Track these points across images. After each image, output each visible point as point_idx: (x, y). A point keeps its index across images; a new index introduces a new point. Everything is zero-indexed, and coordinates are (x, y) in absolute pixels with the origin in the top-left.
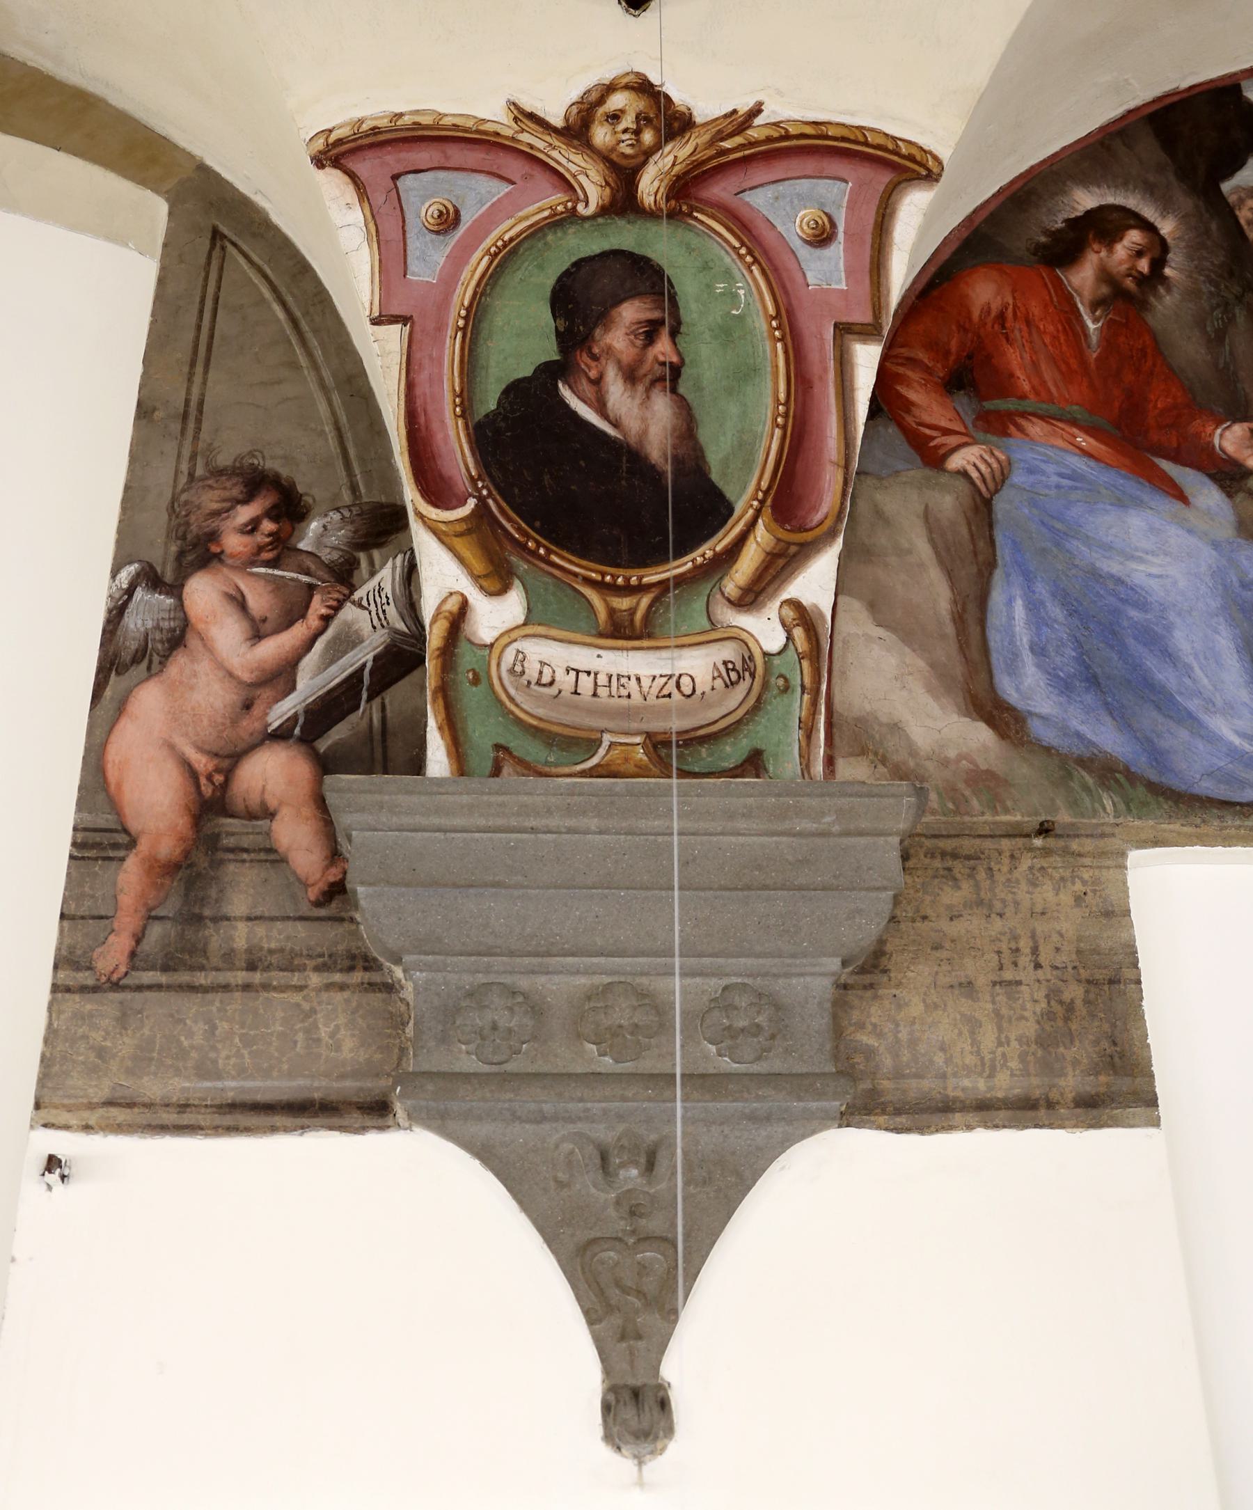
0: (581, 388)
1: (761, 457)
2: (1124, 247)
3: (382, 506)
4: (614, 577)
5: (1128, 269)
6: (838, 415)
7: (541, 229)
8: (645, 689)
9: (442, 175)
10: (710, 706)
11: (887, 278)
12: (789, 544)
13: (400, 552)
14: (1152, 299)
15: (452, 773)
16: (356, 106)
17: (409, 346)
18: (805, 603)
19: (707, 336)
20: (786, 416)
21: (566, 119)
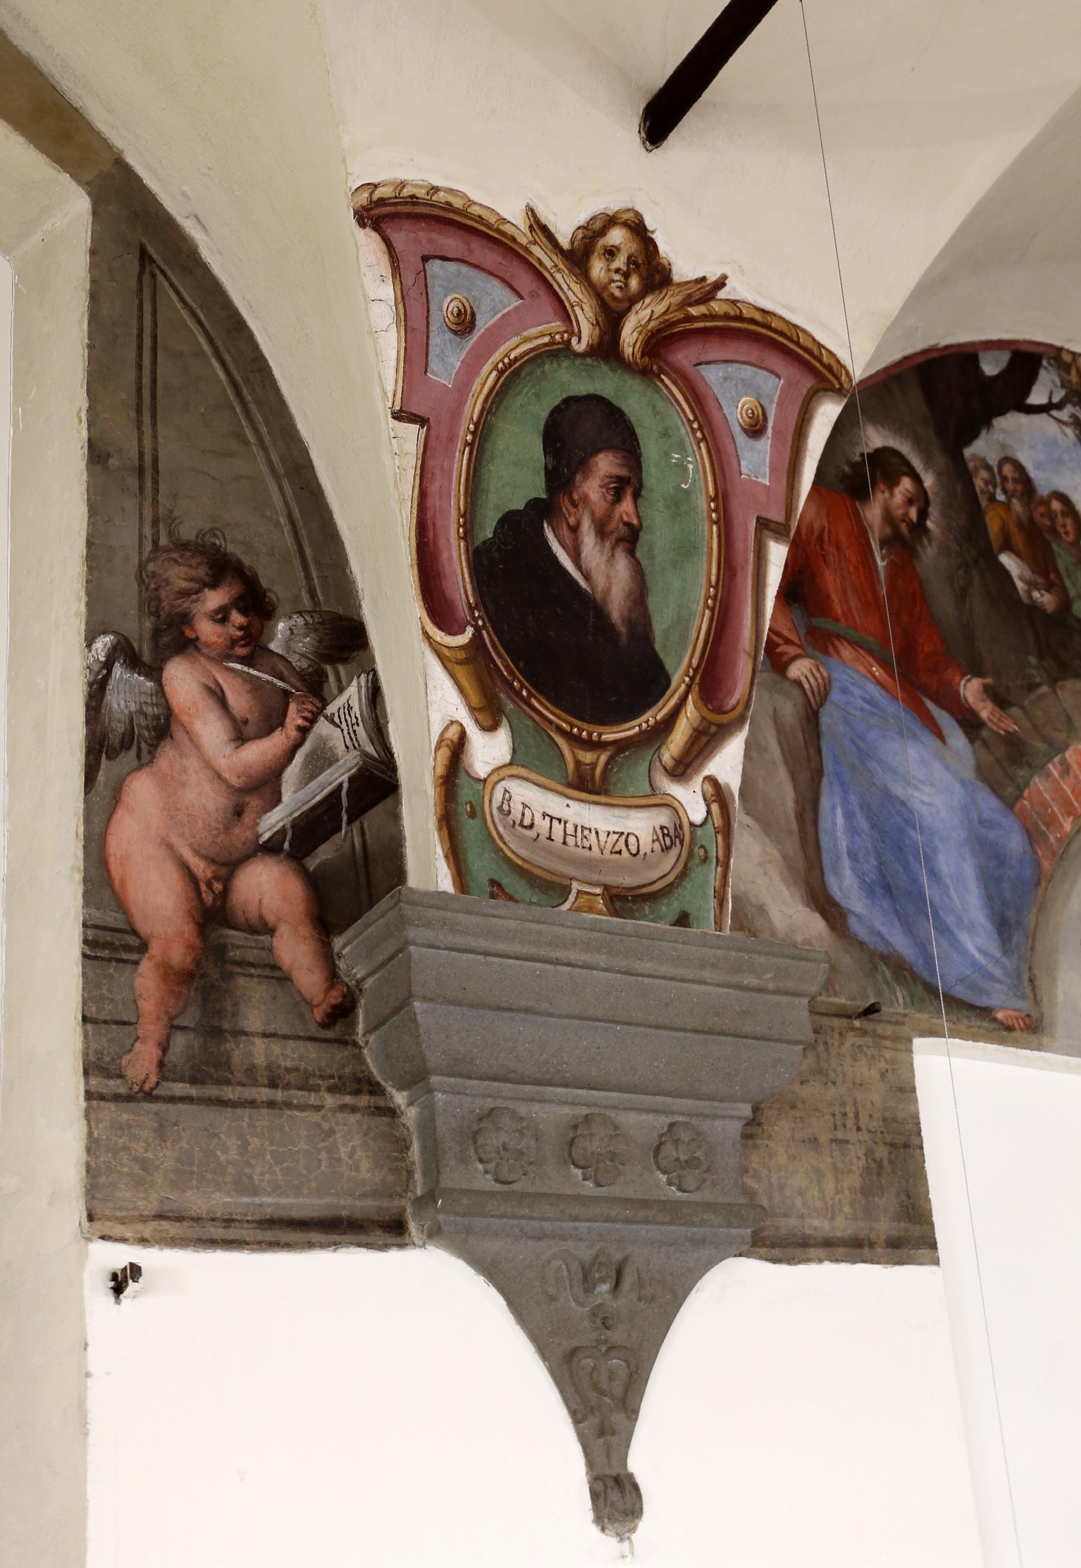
0: (561, 533)
4: (581, 730)
6: (752, 607)
7: (541, 354)
8: (602, 844)
9: (464, 269)
11: (799, 483)
12: (710, 723)
16: (401, 165)
17: (424, 452)
18: (720, 781)
20: (715, 599)
21: (572, 242)
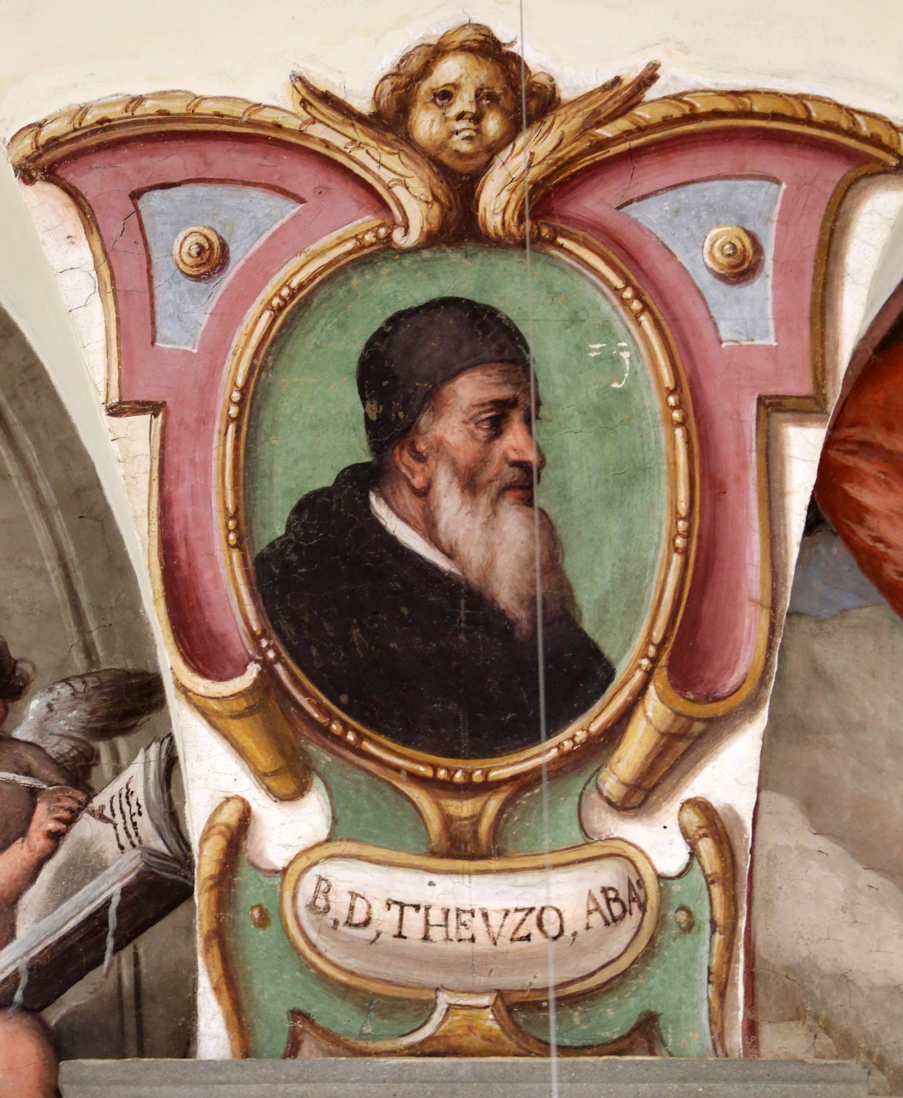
0: (400, 502)
1: (652, 595)
3: (128, 674)
4: (451, 771)
6: (762, 533)
7: (342, 270)
8: (495, 929)
9: (201, 190)
10: (584, 952)
11: (835, 327)
12: (692, 719)
13: (155, 740)
15: (233, 1051)
16: (76, 86)
17: (163, 447)
18: (715, 804)
19: (577, 422)
20: (688, 535)
21: (376, 100)
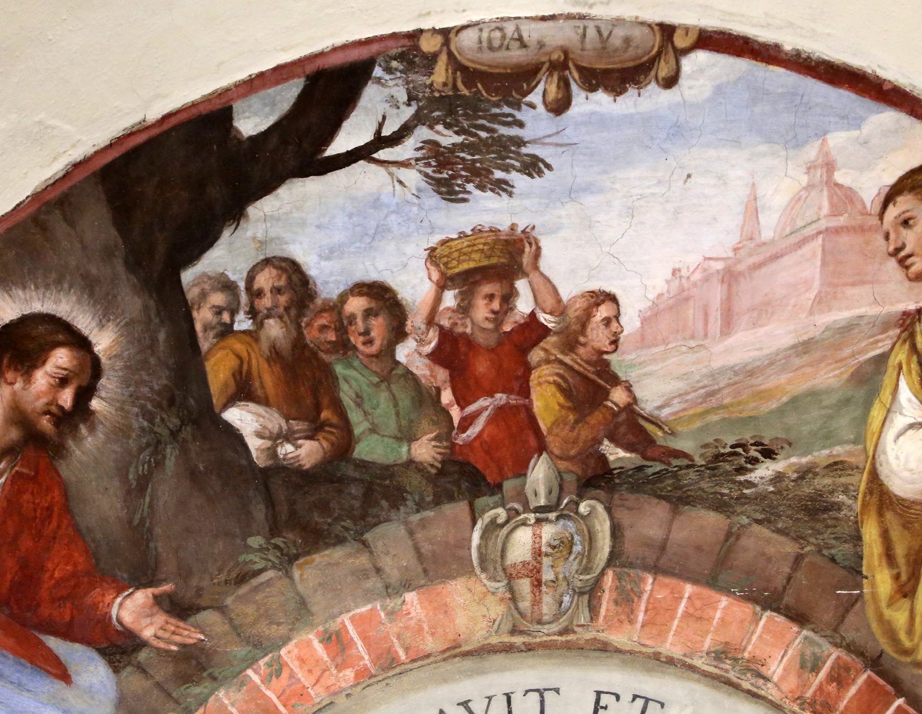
2: (46, 373)
5: (48, 404)
14: (70, 443)
